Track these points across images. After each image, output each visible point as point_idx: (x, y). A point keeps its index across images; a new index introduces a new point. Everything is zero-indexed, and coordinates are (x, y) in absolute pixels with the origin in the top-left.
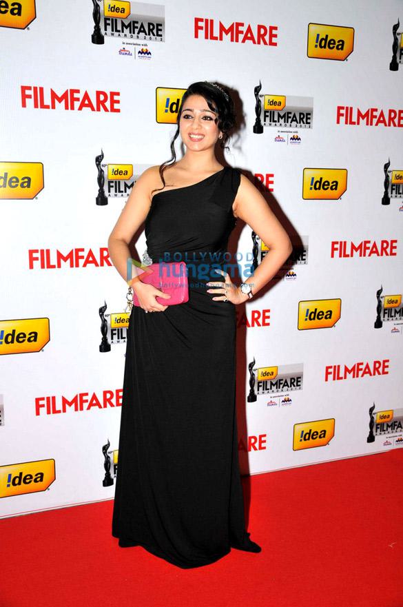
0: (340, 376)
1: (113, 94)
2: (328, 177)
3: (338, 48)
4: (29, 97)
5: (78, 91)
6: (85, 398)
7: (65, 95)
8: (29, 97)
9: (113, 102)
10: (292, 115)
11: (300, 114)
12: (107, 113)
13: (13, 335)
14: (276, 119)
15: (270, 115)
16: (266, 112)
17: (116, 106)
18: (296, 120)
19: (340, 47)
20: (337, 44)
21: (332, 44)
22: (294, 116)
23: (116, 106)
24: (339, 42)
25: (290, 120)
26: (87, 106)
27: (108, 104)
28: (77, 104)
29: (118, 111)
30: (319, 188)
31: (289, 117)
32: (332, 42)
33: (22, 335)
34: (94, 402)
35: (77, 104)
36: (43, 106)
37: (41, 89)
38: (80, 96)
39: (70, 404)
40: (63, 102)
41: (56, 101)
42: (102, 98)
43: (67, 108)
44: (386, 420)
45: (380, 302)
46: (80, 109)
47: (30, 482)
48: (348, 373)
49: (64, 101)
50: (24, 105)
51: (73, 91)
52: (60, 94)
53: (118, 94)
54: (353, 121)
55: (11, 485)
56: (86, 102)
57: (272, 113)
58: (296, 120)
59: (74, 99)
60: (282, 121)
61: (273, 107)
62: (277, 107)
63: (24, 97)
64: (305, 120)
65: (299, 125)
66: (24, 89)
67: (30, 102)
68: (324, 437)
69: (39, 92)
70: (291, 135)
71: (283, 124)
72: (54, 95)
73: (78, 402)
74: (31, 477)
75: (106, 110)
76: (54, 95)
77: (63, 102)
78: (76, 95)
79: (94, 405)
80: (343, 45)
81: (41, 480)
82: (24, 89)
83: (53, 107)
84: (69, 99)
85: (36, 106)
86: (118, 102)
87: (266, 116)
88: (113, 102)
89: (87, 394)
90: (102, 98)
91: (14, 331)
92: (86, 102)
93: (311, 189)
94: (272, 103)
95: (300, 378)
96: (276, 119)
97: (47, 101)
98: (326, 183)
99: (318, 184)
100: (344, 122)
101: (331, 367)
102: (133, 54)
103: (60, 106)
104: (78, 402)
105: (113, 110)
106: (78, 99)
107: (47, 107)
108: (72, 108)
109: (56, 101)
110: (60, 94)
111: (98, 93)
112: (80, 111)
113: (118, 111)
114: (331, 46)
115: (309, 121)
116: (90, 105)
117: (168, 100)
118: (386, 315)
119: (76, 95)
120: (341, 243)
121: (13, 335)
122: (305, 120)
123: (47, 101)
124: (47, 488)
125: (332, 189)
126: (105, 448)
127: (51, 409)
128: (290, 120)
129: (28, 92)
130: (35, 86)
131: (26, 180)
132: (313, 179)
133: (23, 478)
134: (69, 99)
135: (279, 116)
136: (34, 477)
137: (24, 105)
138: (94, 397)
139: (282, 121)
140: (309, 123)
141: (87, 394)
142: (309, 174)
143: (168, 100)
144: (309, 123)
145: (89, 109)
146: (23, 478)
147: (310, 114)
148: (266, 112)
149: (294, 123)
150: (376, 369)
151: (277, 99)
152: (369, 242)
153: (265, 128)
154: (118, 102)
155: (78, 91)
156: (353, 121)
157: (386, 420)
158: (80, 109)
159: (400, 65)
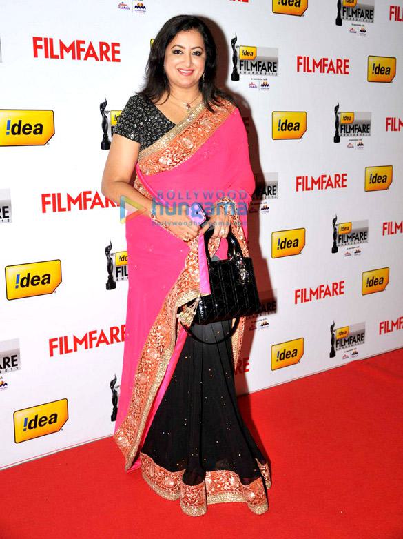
1: (114, 45)
2: (292, 119)
5: (83, 42)
6: (94, 336)
7: (72, 46)
9: (114, 52)
10: (261, 64)
11: (269, 63)
12: (109, 62)
14: (249, 68)
15: (244, 63)
16: (241, 61)
17: (117, 56)
18: (265, 69)
22: (264, 65)
23: (117, 56)
25: (260, 68)
26: (91, 56)
27: (110, 54)
28: (83, 54)
29: (118, 60)
30: (285, 130)
31: (260, 66)
34: (103, 339)
35: (83, 54)
36: (53, 56)
37: (51, 40)
39: (81, 343)
40: (71, 52)
41: (64, 51)
42: (104, 48)
44: (344, 335)
45: (335, 229)
47: (45, 423)
49: (71, 52)
51: (80, 42)
52: (67, 45)
53: (118, 45)
55: (28, 429)
56: (90, 53)
57: (246, 62)
58: (265, 69)
60: (254, 69)
61: (246, 57)
62: (250, 57)
63: (36, 47)
64: (272, 68)
65: (267, 73)
66: (36, 39)
67: (41, 52)
69: (49, 43)
70: (262, 82)
71: (255, 72)
72: (62, 46)
73: (88, 340)
74: (46, 418)
75: (108, 59)
76: (62, 46)
77: (71, 52)
78: (82, 46)
79: (103, 342)
82: (36, 39)
83: (62, 57)
84: (75, 49)
85: (47, 56)
86: (118, 52)
88: (114, 52)
89: (95, 332)
90: (104, 48)
92: (91, 52)
93: (279, 130)
94: (246, 53)
96: (249, 68)
97: (57, 51)
99: (284, 125)
104: (88, 340)
105: (115, 60)
106: (83, 50)
107: (57, 57)
108: (79, 58)
110: (67, 45)
111: (102, 44)
113: (118, 60)
115: (275, 69)
116: (94, 55)
118: (341, 241)
119: (82, 46)
122: (272, 68)
123: (57, 51)
124: (61, 428)
126: (113, 384)
127: (65, 350)
128: (260, 68)
129: (39, 43)
132: (280, 121)
134: (75, 49)
135: (252, 65)
137: (36, 55)
138: (102, 334)
139: (254, 69)
140: (276, 71)
141: (95, 332)
142: (277, 117)
144: (276, 71)
145: (94, 58)
147: (276, 63)
148: (241, 61)
149: (264, 71)
150: (334, 290)
151: (249, 50)
153: (241, 76)
157: (344, 335)
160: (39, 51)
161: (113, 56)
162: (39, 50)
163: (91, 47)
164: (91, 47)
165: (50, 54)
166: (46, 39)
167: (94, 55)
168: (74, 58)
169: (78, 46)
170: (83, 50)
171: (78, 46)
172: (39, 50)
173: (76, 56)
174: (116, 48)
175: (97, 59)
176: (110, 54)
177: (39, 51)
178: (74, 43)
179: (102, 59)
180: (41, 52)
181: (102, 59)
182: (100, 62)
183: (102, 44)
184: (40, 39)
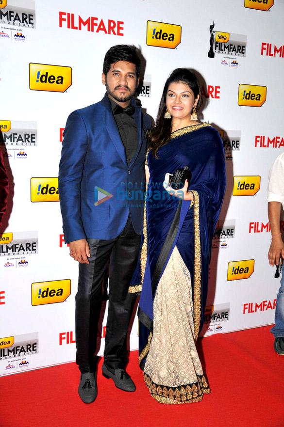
0: (259, 230)
1: (119, 23)
3: (169, 40)
4: (64, 20)
7: (88, 21)
8: (64, 20)
9: (119, 28)
13: (47, 188)
17: (121, 32)
19: (171, 39)
20: (169, 36)
21: (165, 36)
23: (121, 32)
24: (170, 35)
26: (102, 29)
27: (116, 29)
28: (96, 28)
29: (122, 35)
32: (165, 35)
33: (53, 189)
35: (96, 28)
36: (73, 27)
37: (73, 15)
38: (98, 22)
40: (87, 25)
41: (82, 25)
42: (112, 25)
43: (89, 30)
46: (98, 31)
48: (263, 228)
49: (87, 25)
50: (61, 25)
51: (94, 19)
52: (85, 20)
54: (271, 53)
59: (94, 24)
63: (61, 20)
66: (61, 14)
67: (65, 23)
68: (247, 272)
69: (71, 17)
72: (81, 20)
75: (114, 33)
76: (81, 20)
77: (87, 25)
78: (95, 22)
80: (173, 37)
81: (61, 294)
82: (61, 14)
85: (69, 27)
86: (122, 28)
87: (216, 46)
88: (119, 28)
90: (112, 25)
91: (48, 185)
92: (102, 27)
95: (233, 229)
97: (76, 24)
98: (253, 95)
100: (266, 54)
101: (253, 223)
102: (10, 37)
103: (85, 28)
105: (119, 34)
107: (76, 28)
108: (93, 30)
109: (82, 25)
110: (85, 20)
111: (110, 21)
112: (97, 33)
113: (122, 35)
114: (165, 38)
116: (104, 29)
117: (155, 30)
119: (95, 22)
120: (261, 137)
121: (47, 188)
123: (76, 24)
125: (257, 100)
130: (69, 12)
131: (60, 78)
133: (49, 291)
136: (57, 292)
137: (61, 25)
143: (155, 30)
145: (103, 32)
146: (49, 291)
152: (279, 138)
154: (122, 28)
155: (96, 19)
156: (271, 53)
158: (98, 31)
159: (215, 54)
160: (63, 22)
161: (118, 31)
162: (63, 22)
163: (102, 23)
164: (102, 23)
165: (71, 25)
166: (69, 14)
167: (104, 29)
168: (89, 30)
169: (92, 22)
170: (96, 24)
171: (92, 22)
172: (63, 22)
173: (90, 29)
174: (121, 26)
175: (106, 32)
176: (116, 29)
177: (63, 22)
178: (89, 18)
179: (110, 33)
180: (65, 23)
181: (110, 33)
182: (108, 35)
183: (110, 21)
184: (65, 14)
